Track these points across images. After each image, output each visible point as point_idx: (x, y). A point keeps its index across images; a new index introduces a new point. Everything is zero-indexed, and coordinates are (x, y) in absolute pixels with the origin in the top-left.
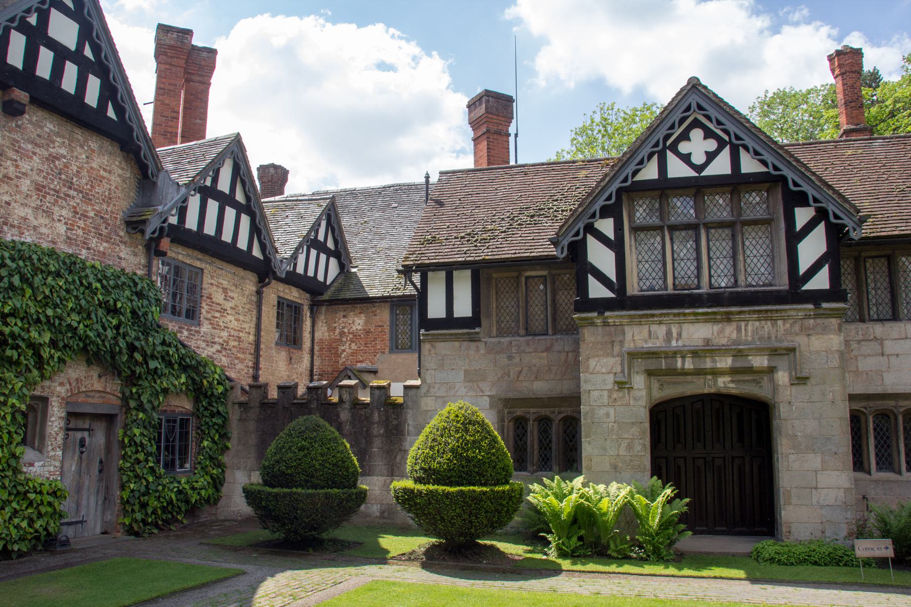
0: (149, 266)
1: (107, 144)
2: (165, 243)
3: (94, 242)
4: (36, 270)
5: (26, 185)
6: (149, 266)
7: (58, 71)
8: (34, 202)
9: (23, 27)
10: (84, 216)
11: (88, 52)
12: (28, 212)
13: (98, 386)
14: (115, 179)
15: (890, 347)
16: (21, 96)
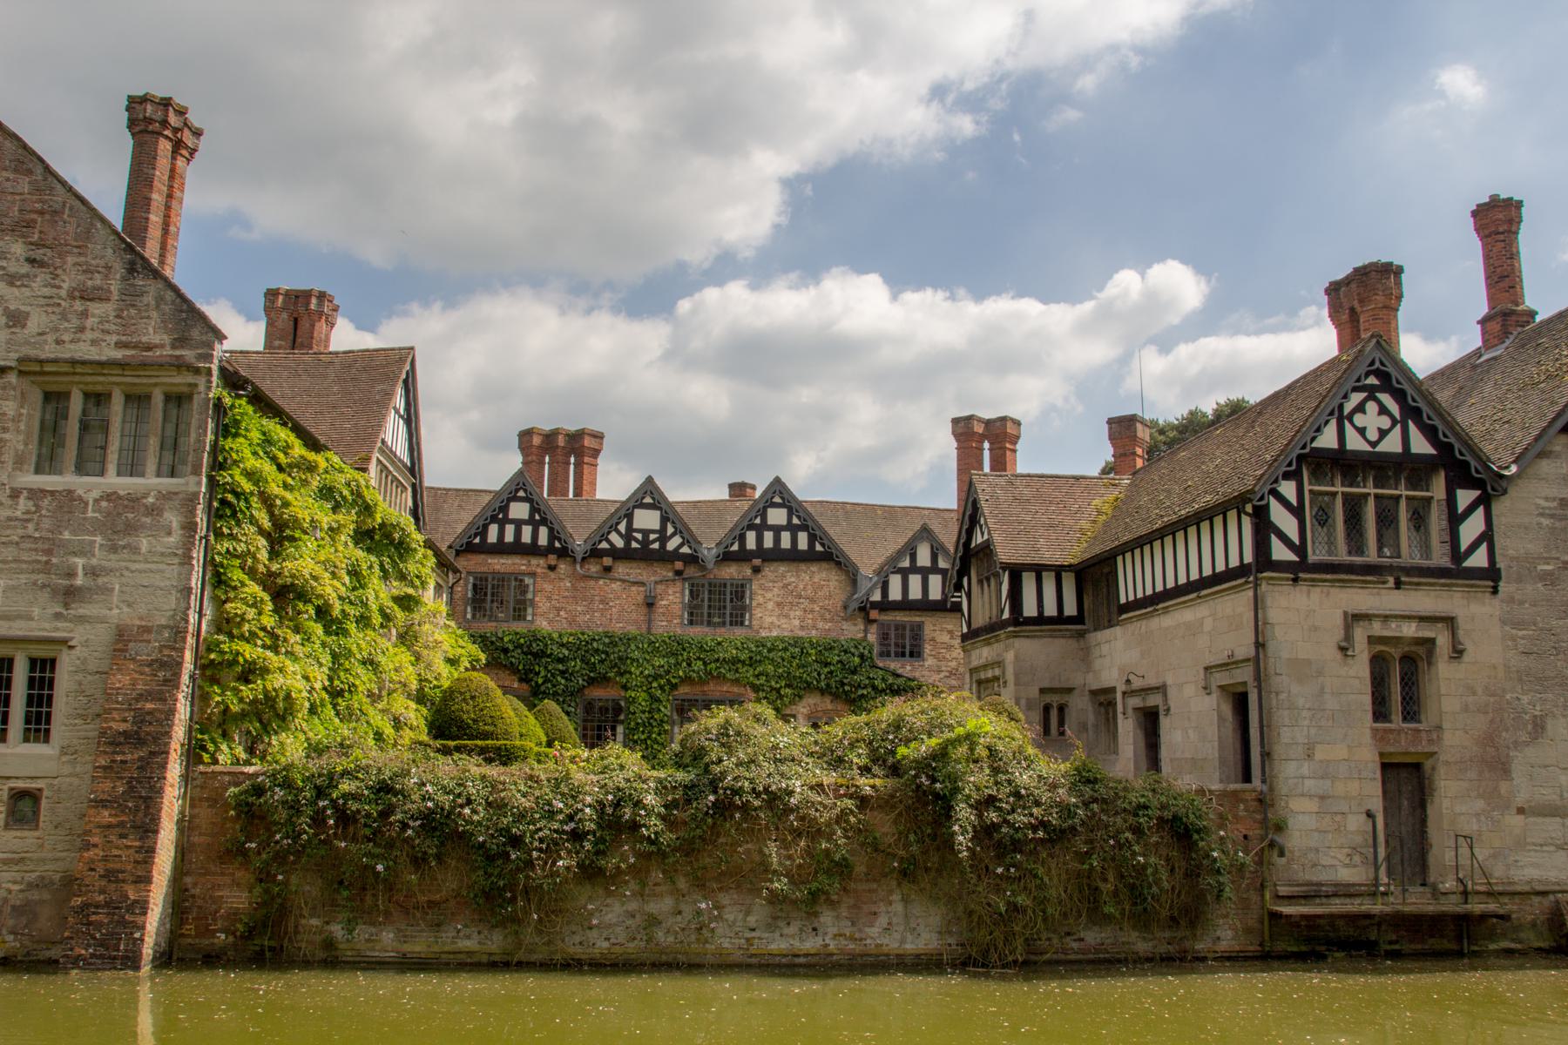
0: (866, 631)
1: (824, 565)
2: (874, 614)
3: (820, 625)
4: (770, 651)
5: (770, 605)
6: (866, 631)
7: (777, 540)
8: (777, 612)
9: (751, 527)
10: (812, 611)
11: (795, 521)
12: (774, 619)
13: (830, 707)
14: (833, 584)
16: (757, 562)
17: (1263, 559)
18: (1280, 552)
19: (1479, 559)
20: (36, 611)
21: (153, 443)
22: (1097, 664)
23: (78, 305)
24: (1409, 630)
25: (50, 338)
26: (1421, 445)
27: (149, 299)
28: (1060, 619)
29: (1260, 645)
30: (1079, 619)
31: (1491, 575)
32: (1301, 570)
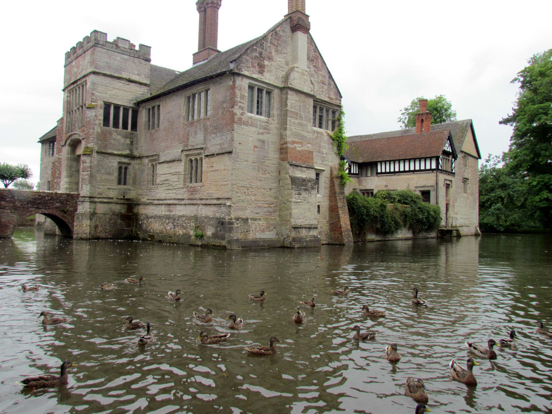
15: (368, 181)
17: (437, 169)
18: (440, 168)
19: (453, 171)
20: (319, 162)
21: (330, 123)
22: (364, 184)
23: (322, 85)
24: (448, 182)
25: (318, 92)
26: (451, 151)
27: (332, 87)
28: (356, 174)
29: (437, 184)
30: (358, 174)
31: (454, 173)
32: (442, 171)
